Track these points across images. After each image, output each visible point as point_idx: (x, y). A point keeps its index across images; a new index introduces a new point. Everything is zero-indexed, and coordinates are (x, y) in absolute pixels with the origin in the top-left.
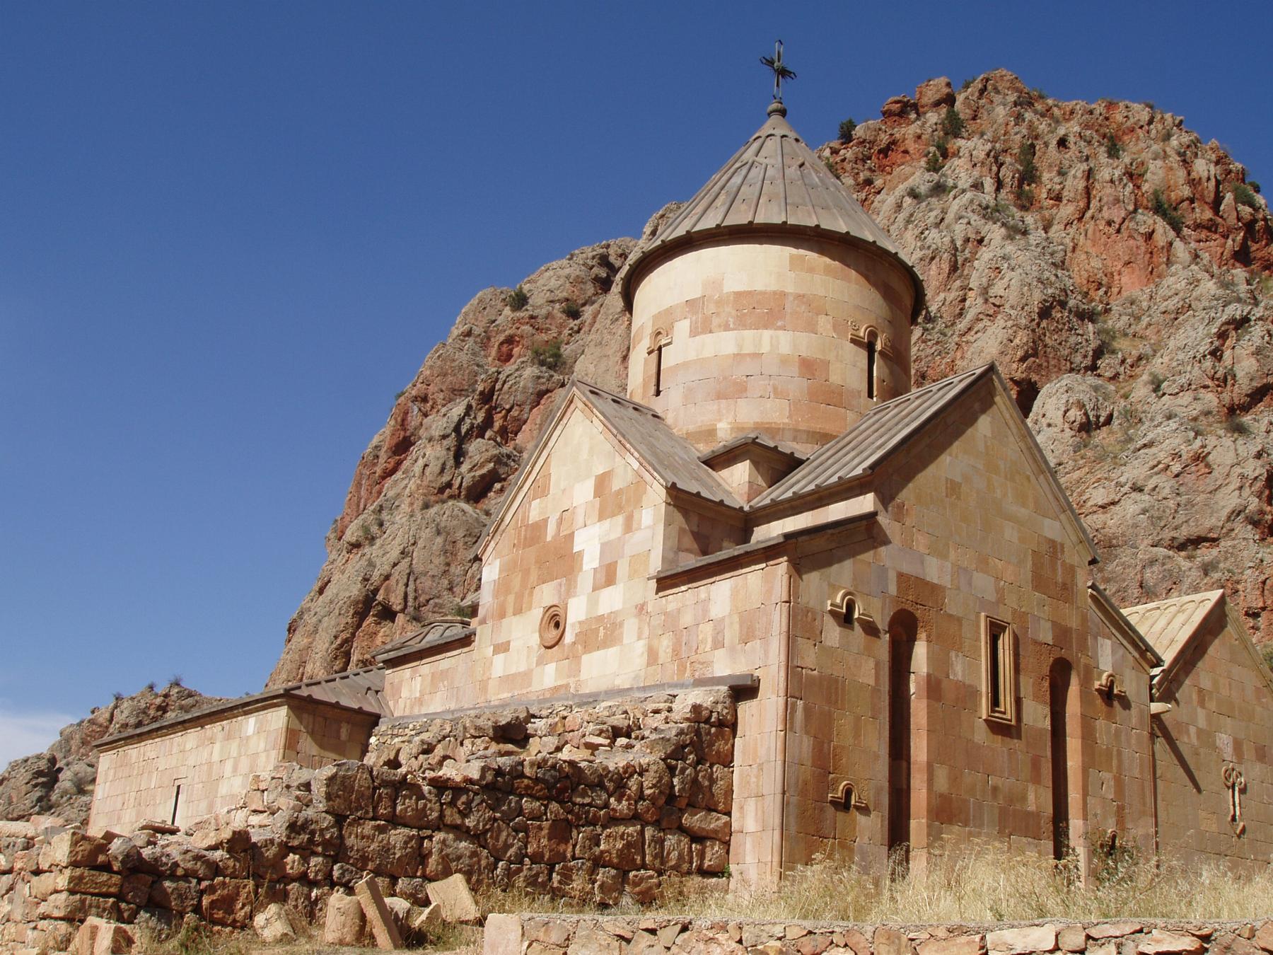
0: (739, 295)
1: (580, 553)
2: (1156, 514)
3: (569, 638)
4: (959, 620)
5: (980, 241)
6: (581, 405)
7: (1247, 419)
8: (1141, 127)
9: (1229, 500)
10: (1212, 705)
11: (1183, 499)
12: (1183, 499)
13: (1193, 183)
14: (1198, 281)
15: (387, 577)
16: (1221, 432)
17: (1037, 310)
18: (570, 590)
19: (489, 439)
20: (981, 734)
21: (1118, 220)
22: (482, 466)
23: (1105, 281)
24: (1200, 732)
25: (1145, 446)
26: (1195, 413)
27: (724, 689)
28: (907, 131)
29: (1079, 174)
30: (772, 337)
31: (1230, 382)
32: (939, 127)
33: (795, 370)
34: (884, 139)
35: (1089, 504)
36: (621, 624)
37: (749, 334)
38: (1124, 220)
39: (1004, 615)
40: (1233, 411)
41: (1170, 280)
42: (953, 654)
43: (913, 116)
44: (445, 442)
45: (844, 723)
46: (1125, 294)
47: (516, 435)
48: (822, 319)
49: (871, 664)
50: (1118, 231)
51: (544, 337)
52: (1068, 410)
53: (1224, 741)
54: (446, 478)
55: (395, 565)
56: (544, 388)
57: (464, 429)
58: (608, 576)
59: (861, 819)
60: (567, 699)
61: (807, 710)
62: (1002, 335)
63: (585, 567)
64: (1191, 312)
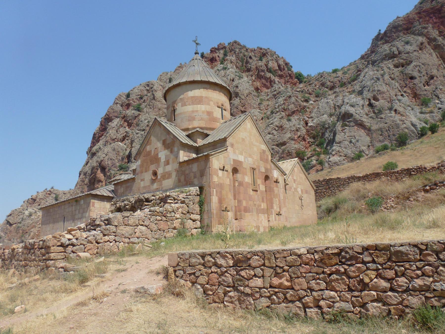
0: (192, 97)
1: (160, 158)
2: (273, 139)
3: (159, 177)
4: (246, 169)
5: (233, 80)
6: (157, 124)
7: (291, 118)
9: (288, 135)
10: (296, 183)
11: (278, 135)
12: (278, 135)
13: (279, 66)
14: (280, 88)
15: (102, 161)
16: (286, 121)
18: (158, 166)
19: (125, 127)
20: (252, 193)
21: (263, 75)
22: (123, 134)
23: (260, 88)
24: (294, 188)
25: (270, 124)
26: (280, 117)
27: (198, 187)
28: (216, 55)
29: (254, 65)
31: (288, 110)
32: (222, 54)
34: (211, 57)
36: (171, 174)
37: (195, 106)
39: (255, 167)
40: (289, 115)
42: (245, 176)
43: (217, 51)
44: (114, 129)
45: (224, 192)
46: (264, 91)
47: (131, 126)
49: (229, 180)
51: (136, 104)
53: (299, 190)
54: (115, 137)
55: (104, 158)
56: (136, 115)
57: (118, 125)
58: (167, 163)
59: (229, 213)
60: (160, 191)
61: (216, 191)
62: (239, 101)
63: (162, 161)
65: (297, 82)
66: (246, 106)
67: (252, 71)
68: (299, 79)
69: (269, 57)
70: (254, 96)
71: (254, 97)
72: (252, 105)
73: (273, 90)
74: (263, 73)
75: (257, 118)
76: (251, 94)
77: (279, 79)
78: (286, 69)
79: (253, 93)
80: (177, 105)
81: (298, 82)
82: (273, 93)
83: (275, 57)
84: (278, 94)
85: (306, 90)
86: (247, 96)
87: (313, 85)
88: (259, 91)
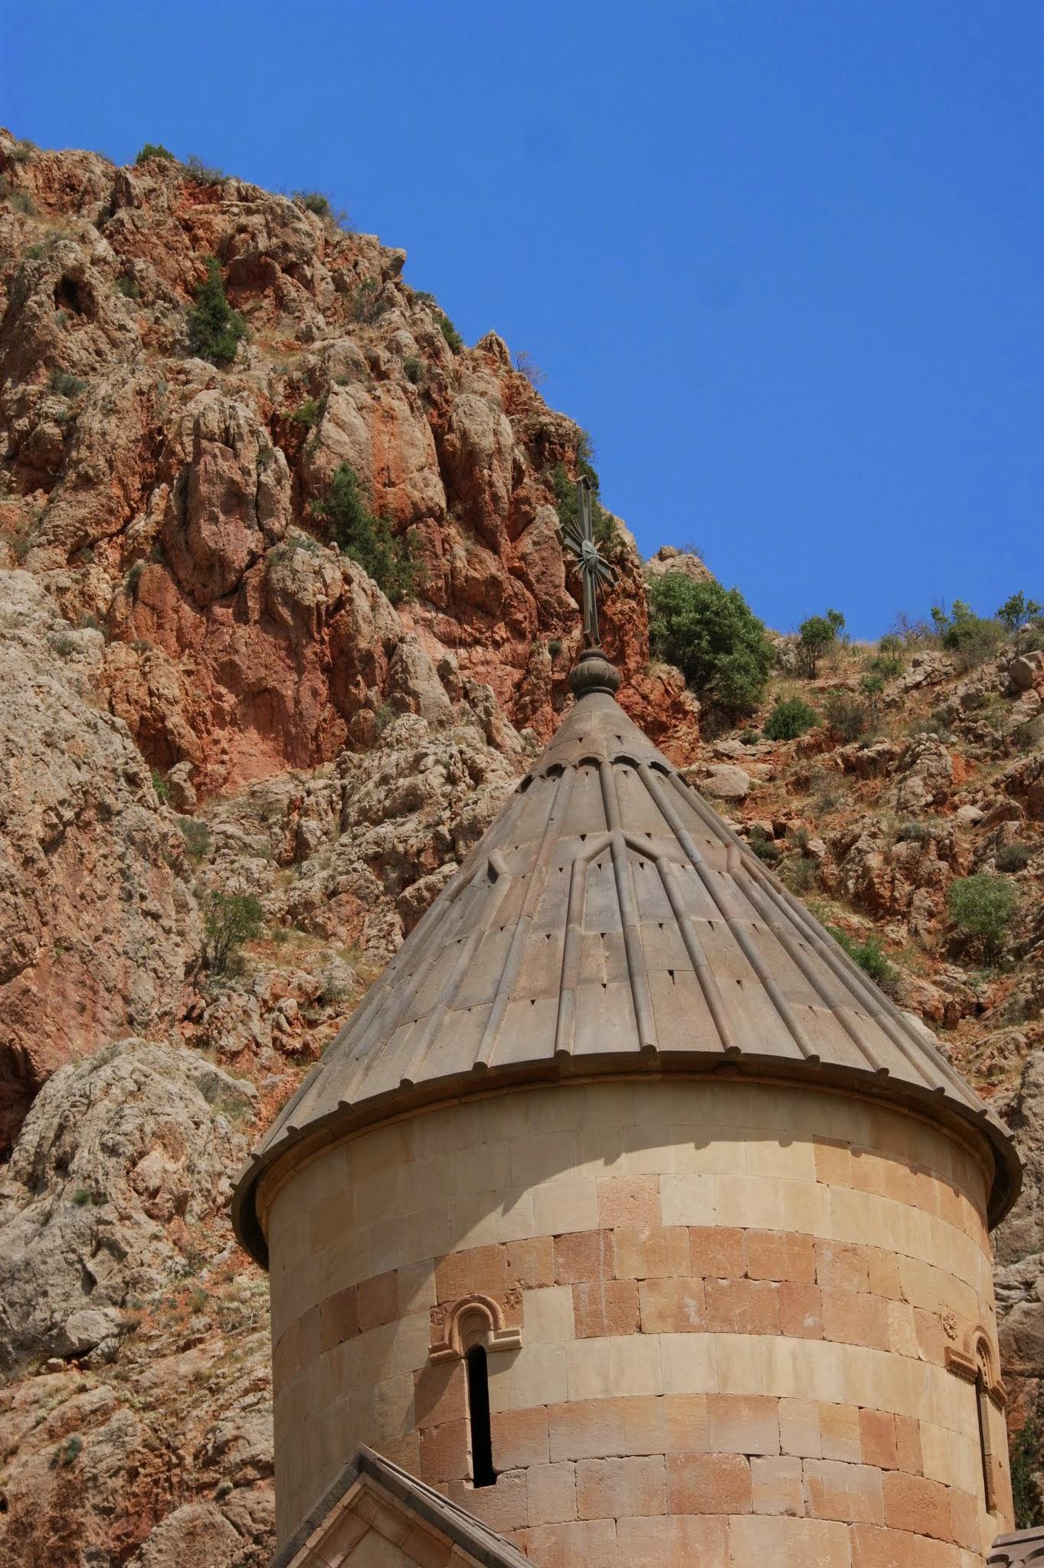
0: (701, 1236)
6: (388, 1526)
8: (290, 269)
14: (477, 776)
17: (38, 830)
23: (188, 738)
30: (795, 1357)
33: (853, 1444)
35: (233, 1457)
37: (743, 1342)
38: (254, 558)
41: (393, 759)
48: (896, 1313)
50: (235, 592)
52: (142, 1155)
64: (450, 868)
65: (678, 708)
66: (28, 979)
67: (87, 482)
68: (696, 675)
69: (313, 317)
70: (146, 847)
71: (138, 866)
72: (114, 970)
73: (372, 795)
74: (252, 539)
75: (190, 1169)
76: (106, 813)
77: (450, 642)
78: (548, 517)
79: (133, 815)
80: (514, 1300)
81: (694, 706)
82: (372, 833)
83: (406, 336)
84: (445, 848)
85: (816, 845)
86: (50, 846)
87: (916, 783)
88: (180, 772)
